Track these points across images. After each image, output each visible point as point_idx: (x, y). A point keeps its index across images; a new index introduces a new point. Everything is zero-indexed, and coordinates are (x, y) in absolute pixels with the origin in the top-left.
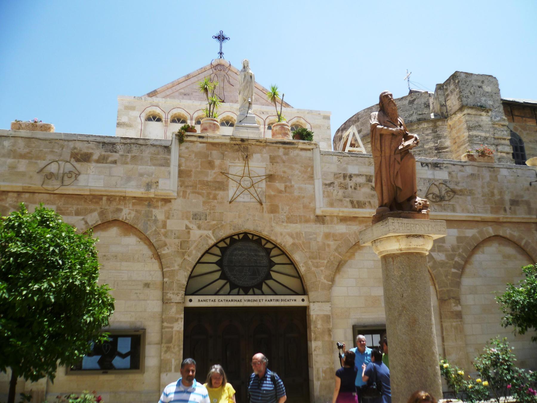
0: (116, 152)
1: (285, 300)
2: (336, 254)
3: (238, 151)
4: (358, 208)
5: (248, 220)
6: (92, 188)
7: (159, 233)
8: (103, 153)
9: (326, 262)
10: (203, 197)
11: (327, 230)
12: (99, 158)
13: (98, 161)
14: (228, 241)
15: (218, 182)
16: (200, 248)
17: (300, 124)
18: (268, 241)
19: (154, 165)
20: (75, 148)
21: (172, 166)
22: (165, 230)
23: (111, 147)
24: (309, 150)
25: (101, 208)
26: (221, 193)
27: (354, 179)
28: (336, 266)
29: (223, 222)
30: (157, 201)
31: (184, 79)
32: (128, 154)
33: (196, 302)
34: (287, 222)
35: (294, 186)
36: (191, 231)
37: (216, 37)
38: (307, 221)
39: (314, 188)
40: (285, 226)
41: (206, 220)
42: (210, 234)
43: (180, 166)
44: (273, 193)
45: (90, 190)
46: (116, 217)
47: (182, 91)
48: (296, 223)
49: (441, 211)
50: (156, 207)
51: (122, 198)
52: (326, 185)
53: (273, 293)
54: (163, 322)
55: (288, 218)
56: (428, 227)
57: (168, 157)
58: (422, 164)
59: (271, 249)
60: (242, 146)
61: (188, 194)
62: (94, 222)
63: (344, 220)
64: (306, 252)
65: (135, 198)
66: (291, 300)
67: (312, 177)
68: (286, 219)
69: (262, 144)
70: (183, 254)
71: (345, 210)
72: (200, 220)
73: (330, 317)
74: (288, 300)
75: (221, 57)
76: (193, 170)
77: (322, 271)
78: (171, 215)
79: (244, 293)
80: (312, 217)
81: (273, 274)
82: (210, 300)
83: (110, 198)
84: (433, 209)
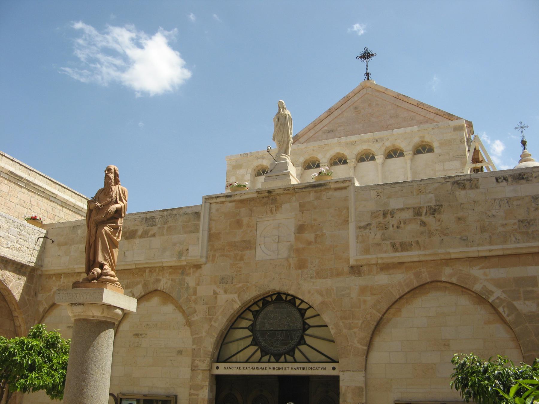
0: (155, 225)
1: (313, 369)
2: (374, 312)
3: (266, 204)
4: (402, 251)
5: (274, 279)
6: (136, 262)
7: (190, 301)
8: (145, 228)
9: (360, 322)
13: (141, 237)
17: (426, 143)
18: (302, 301)
19: (185, 233)
21: (201, 231)
22: (195, 297)
23: (152, 220)
24: (345, 188)
25: (145, 280)
28: (373, 327)
29: (248, 284)
30: (190, 268)
31: (326, 115)
32: (164, 226)
33: (223, 369)
36: (219, 296)
37: (360, 57)
38: (339, 274)
39: (348, 234)
40: (314, 282)
41: (232, 283)
42: (236, 298)
43: (210, 229)
44: (301, 246)
45: (135, 264)
46: (155, 287)
47: (326, 128)
48: (327, 278)
49: (528, 241)
50: (188, 274)
51: (161, 268)
52: (360, 228)
53: (306, 361)
54: (190, 389)
55: (317, 273)
56: (87, 295)
57: (198, 222)
58: (497, 180)
59: (306, 310)
60: (271, 198)
61: (216, 257)
62: (139, 294)
63: (386, 267)
64: (336, 311)
65: (171, 267)
66: (320, 369)
67: (348, 220)
68: (315, 274)
69: (289, 192)
70: (211, 320)
71: (384, 255)
72: (227, 283)
73: (363, 389)
74: (317, 369)
75: (368, 79)
77: (355, 333)
79: (275, 361)
80: (346, 269)
81: (306, 338)
82: (235, 367)
83: (152, 270)
84: (513, 239)
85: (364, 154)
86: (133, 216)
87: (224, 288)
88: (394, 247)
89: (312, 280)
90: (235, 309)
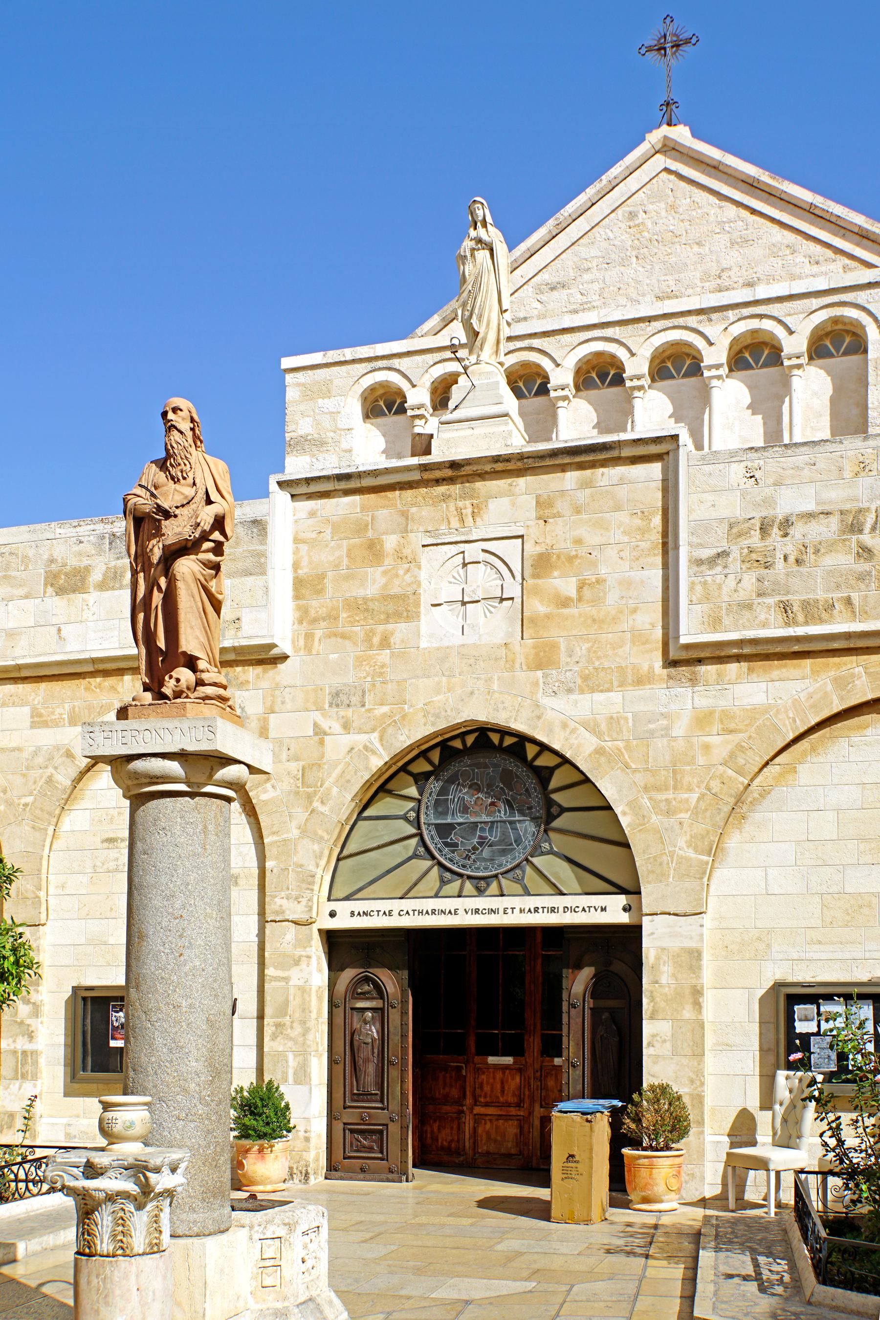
3: (446, 498)
5: (472, 693)
10: (355, 644)
11: (703, 702)
12: (105, 575)
13: (102, 586)
14: (435, 756)
15: (394, 597)
16: (349, 781)
18: (544, 748)
20: (52, 561)
26: (400, 630)
27: (798, 531)
34: (582, 692)
35: (605, 580)
36: (327, 738)
38: (640, 681)
41: (363, 706)
43: (296, 566)
52: (699, 562)
55: (585, 678)
61: (317, 640)
68: (579, 681)
72: (348, 706)
76: (329, 574)
78: (279, 699)
85: (669, 358)
86: (74, 530)
87: (343, 717)
88: (786, 612)
89: (573, 697)
90: (375, 770)
